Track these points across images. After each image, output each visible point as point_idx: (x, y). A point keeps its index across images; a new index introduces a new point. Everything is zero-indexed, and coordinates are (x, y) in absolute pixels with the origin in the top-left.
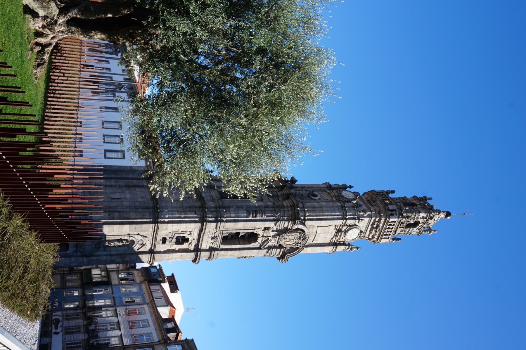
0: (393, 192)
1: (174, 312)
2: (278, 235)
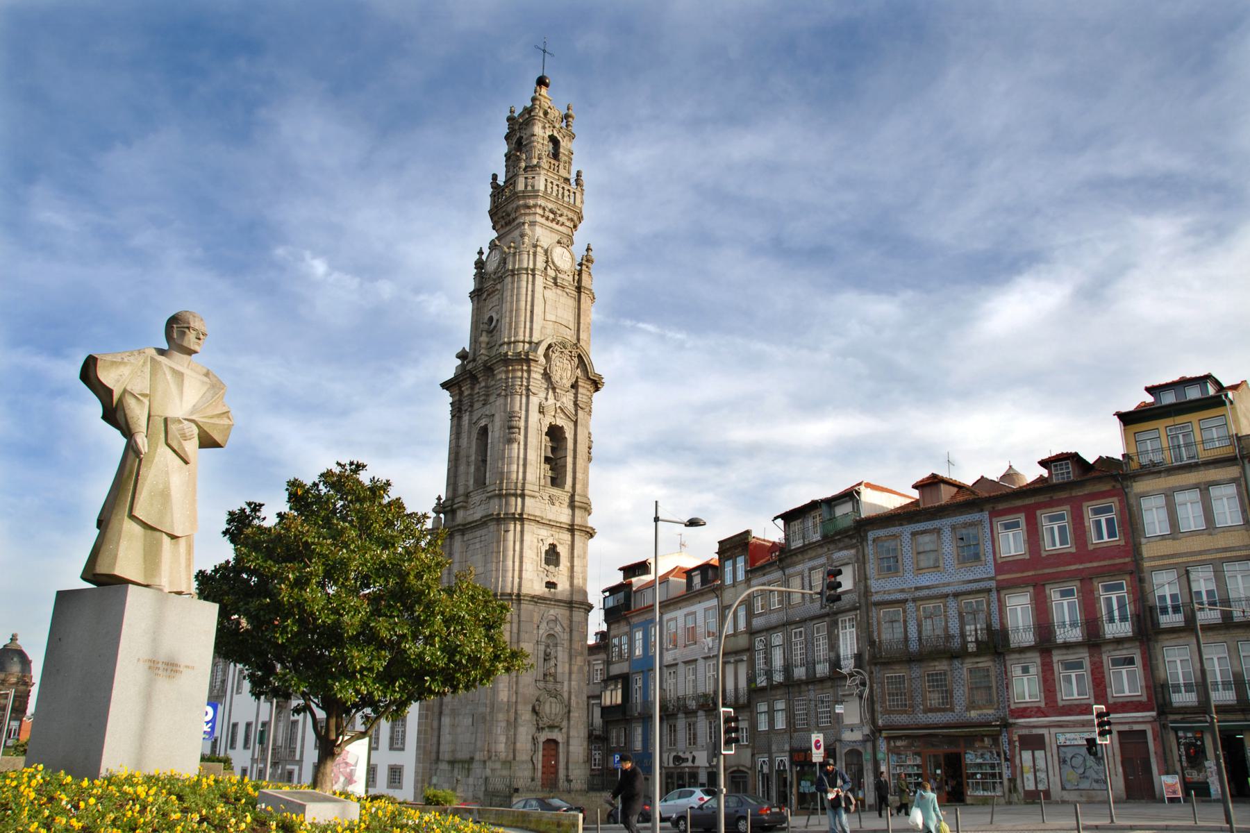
0: (495, 177)
1: (681, 568)
2: (554, 389)
